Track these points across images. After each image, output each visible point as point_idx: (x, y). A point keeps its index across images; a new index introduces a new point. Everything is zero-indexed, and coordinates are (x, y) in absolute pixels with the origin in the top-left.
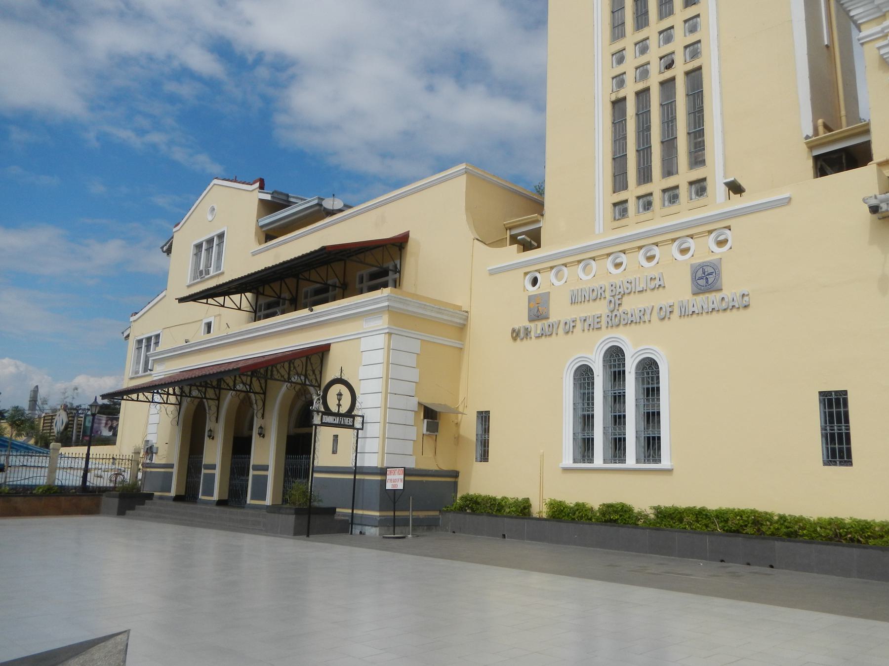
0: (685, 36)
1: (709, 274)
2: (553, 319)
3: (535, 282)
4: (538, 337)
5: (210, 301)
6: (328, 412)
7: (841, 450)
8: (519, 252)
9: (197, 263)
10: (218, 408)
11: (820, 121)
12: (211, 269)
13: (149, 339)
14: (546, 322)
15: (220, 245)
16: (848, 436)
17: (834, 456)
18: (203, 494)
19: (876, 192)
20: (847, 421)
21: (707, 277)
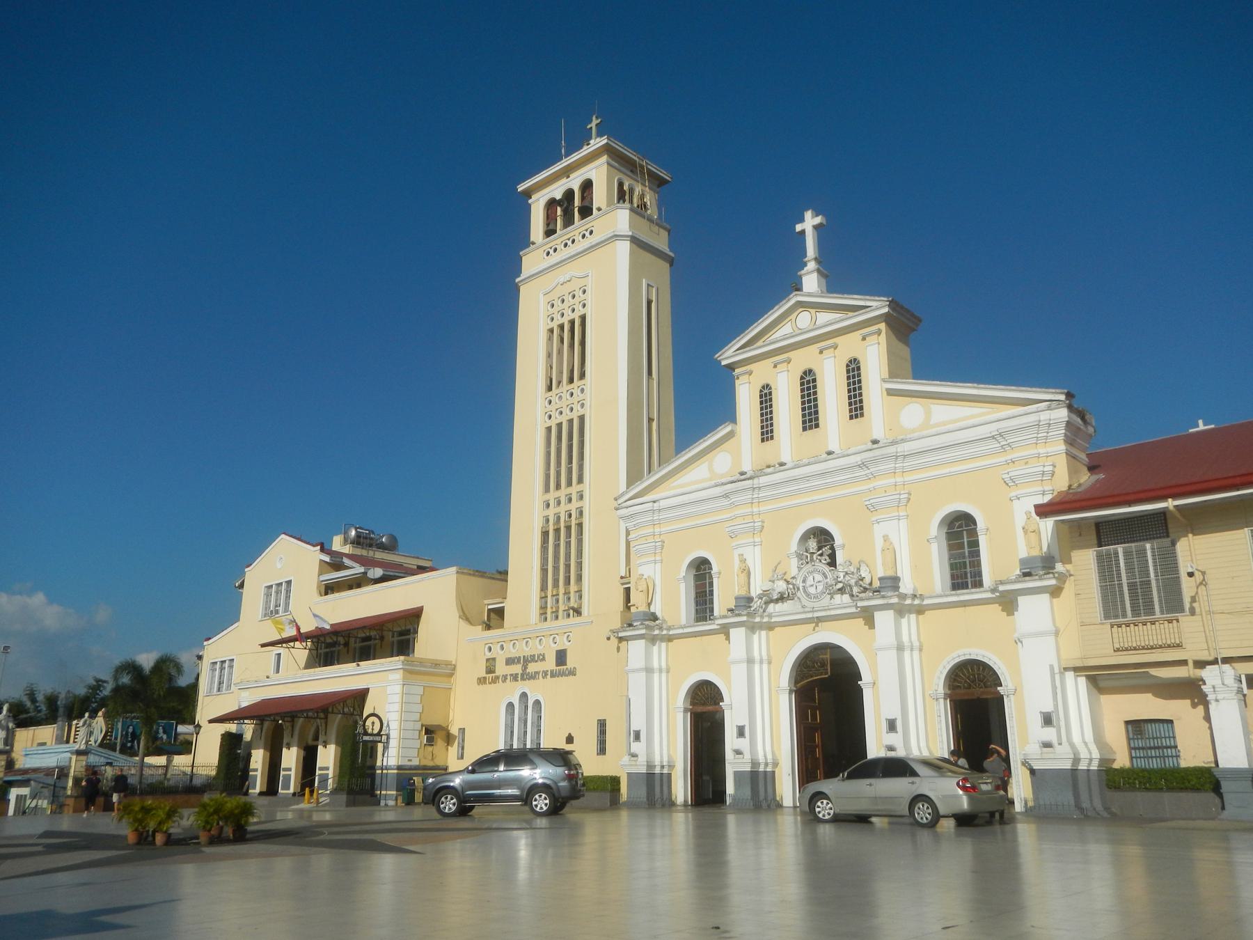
2: (497, 674)
3: (490, 649)
4: (490, 683)
5: (284, 645)
6: (366, 733)
8: (482, 630)
9: (267, 602)
10: (293, 727)
12: (281, 609)
13: (223, 662)
14: (493, 675)
15: (288, 591)
17: (600, 751)
18: (282, 789)
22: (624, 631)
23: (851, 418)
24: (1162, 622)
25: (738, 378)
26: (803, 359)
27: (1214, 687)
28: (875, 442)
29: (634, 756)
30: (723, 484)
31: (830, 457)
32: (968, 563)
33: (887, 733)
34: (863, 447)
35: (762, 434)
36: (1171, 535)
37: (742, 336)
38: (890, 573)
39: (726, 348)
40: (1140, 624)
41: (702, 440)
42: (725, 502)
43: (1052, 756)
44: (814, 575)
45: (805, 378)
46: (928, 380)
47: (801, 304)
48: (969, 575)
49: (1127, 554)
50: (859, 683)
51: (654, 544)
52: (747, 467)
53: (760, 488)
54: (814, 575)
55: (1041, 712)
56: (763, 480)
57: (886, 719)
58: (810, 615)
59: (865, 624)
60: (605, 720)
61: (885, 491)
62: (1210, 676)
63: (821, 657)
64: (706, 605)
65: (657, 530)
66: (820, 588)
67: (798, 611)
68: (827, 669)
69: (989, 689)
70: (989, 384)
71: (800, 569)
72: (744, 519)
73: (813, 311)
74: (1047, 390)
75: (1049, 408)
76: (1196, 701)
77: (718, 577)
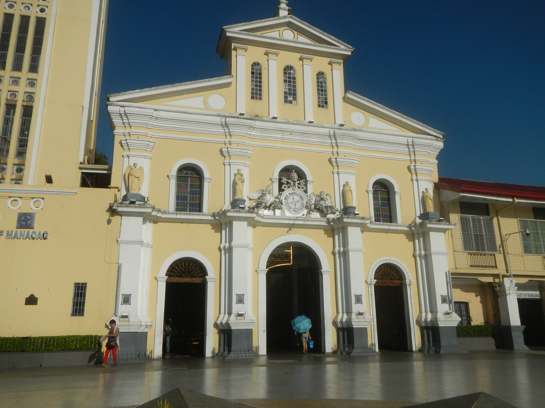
0: (26, 86)
1: (28, 220)
7: (80, 309)
11: (86, 157)
16: (84, 303)
19: (113, 202)
20: (84, 296)
21: (27, 221)
22: (127, 207)
23: (319, 106)
24: (488, 255)
25: (235, 49)
26: (292, 59)
27: (510, 288)
28: (342, 125)
29: (126, 317)
30: (226, 117)
31: (311, 124)
32: (380, 208)
33: (355, 304)
34: (332, 125)
35: (252, 93)
36: (490, 215)
37: (247, 23)
38: (349, 204)
39: (234, 25)
40: (479, 255)
41: (207, 80)
42: (221, 130)
43: (451, 319)
44: (295, 197)
45: (288, 71)
46: (377, 102)
47: (290, 25)
48: (381, 215)
49: (473, 220)
50: (322, 270)
51: (148, 143)
52: (241, 110)
53: (255, 128)
54: (294, 196)
55: (441, 296)
56: (258, 123)
57: (355, 295)
58: (292, 222)
59: (325, 234)
60: (86, 284)
61: (345, 156)
62: (507, 282)
63: (285, 251)
64: (187, 200)
65: (150, 133)
66: (298, 205)
67: (285, 218)
68: (291, 260)
69: (393, 281)
70: (409, 117)
71: (281, 190)
72: (238, 146)
73: (296, 33)
74: (436, 130)
75: (437, 140)
76: (477, 293)
77: (209, 182)
